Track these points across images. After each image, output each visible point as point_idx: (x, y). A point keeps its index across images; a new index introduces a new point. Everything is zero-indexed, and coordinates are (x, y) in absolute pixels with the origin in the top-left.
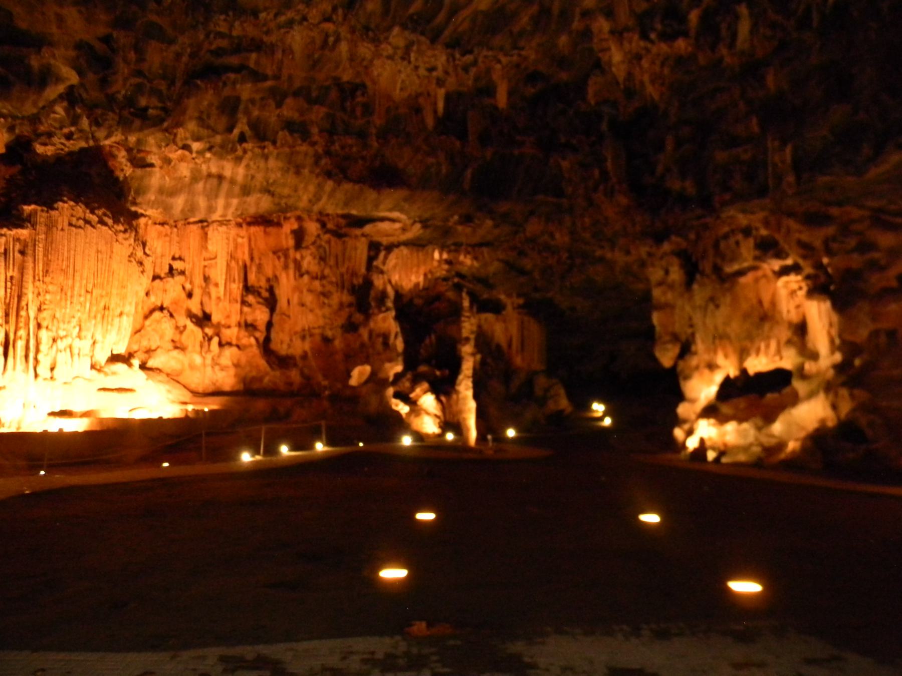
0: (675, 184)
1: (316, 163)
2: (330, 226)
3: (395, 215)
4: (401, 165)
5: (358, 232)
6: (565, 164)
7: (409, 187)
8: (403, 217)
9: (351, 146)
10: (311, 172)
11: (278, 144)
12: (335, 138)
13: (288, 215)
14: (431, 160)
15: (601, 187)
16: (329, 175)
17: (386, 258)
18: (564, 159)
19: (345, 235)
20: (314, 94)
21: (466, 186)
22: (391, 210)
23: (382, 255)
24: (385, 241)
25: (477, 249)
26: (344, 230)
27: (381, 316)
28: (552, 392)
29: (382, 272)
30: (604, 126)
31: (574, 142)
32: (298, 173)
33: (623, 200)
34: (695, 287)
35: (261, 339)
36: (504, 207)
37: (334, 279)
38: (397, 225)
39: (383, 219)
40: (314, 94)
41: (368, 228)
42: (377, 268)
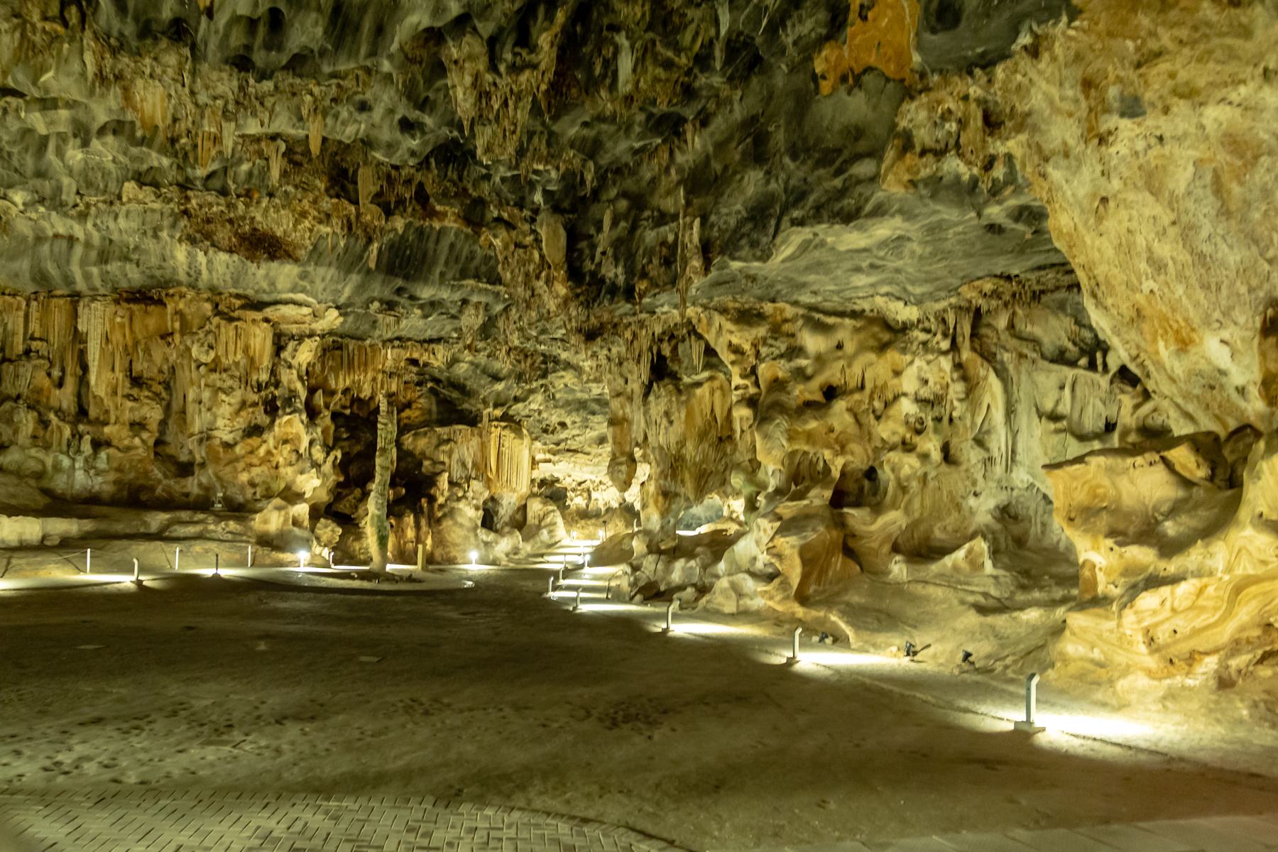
0: (614, 272)
1: (173, 226)
2: (221, 307)
3: (300, 297)
4: (279, 233)
5: (258, 316)
6: (497, 242)
7: (296, 260)
8: (310, 300)
9: (211, 205)
10: (172, 237)
11: (125, 199)
12: (190, 193)
13: (171, 291)
14: (325, 229)
15: (543, 274)
16: (192, 241)
17: (296, 350)
18: (495, 236)
19: (239, 319)
20: (139, 134)
21: (372, 265)
22: (293, 290)
23: (291, 345)
24: (294, 329)
25: (426, 345)
26: (236, 314)
27: (286, 418)
28: (548, 520)
29: (290, 367)
30: (538, 197)
31: (505, 215)
32: (156, 236)
33: (561, 290)
34: (651, 398)
35: (151, 442)
36: (426, 293)
37: (238, 374)
38: (305, 310)
39: (286, 303)
40: (139, 134)
41: (269, 312)
42: (286, 361)
